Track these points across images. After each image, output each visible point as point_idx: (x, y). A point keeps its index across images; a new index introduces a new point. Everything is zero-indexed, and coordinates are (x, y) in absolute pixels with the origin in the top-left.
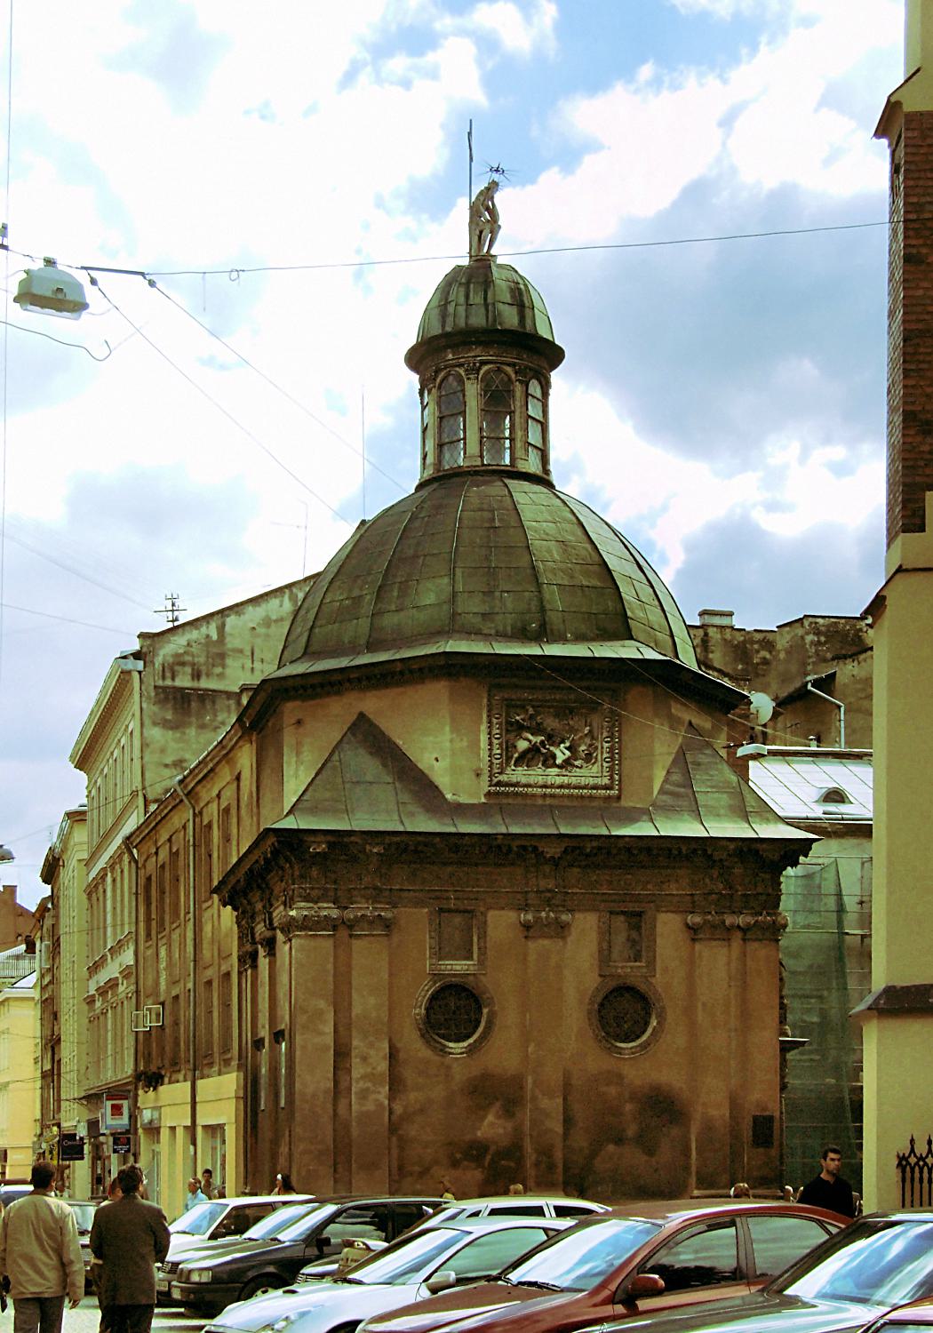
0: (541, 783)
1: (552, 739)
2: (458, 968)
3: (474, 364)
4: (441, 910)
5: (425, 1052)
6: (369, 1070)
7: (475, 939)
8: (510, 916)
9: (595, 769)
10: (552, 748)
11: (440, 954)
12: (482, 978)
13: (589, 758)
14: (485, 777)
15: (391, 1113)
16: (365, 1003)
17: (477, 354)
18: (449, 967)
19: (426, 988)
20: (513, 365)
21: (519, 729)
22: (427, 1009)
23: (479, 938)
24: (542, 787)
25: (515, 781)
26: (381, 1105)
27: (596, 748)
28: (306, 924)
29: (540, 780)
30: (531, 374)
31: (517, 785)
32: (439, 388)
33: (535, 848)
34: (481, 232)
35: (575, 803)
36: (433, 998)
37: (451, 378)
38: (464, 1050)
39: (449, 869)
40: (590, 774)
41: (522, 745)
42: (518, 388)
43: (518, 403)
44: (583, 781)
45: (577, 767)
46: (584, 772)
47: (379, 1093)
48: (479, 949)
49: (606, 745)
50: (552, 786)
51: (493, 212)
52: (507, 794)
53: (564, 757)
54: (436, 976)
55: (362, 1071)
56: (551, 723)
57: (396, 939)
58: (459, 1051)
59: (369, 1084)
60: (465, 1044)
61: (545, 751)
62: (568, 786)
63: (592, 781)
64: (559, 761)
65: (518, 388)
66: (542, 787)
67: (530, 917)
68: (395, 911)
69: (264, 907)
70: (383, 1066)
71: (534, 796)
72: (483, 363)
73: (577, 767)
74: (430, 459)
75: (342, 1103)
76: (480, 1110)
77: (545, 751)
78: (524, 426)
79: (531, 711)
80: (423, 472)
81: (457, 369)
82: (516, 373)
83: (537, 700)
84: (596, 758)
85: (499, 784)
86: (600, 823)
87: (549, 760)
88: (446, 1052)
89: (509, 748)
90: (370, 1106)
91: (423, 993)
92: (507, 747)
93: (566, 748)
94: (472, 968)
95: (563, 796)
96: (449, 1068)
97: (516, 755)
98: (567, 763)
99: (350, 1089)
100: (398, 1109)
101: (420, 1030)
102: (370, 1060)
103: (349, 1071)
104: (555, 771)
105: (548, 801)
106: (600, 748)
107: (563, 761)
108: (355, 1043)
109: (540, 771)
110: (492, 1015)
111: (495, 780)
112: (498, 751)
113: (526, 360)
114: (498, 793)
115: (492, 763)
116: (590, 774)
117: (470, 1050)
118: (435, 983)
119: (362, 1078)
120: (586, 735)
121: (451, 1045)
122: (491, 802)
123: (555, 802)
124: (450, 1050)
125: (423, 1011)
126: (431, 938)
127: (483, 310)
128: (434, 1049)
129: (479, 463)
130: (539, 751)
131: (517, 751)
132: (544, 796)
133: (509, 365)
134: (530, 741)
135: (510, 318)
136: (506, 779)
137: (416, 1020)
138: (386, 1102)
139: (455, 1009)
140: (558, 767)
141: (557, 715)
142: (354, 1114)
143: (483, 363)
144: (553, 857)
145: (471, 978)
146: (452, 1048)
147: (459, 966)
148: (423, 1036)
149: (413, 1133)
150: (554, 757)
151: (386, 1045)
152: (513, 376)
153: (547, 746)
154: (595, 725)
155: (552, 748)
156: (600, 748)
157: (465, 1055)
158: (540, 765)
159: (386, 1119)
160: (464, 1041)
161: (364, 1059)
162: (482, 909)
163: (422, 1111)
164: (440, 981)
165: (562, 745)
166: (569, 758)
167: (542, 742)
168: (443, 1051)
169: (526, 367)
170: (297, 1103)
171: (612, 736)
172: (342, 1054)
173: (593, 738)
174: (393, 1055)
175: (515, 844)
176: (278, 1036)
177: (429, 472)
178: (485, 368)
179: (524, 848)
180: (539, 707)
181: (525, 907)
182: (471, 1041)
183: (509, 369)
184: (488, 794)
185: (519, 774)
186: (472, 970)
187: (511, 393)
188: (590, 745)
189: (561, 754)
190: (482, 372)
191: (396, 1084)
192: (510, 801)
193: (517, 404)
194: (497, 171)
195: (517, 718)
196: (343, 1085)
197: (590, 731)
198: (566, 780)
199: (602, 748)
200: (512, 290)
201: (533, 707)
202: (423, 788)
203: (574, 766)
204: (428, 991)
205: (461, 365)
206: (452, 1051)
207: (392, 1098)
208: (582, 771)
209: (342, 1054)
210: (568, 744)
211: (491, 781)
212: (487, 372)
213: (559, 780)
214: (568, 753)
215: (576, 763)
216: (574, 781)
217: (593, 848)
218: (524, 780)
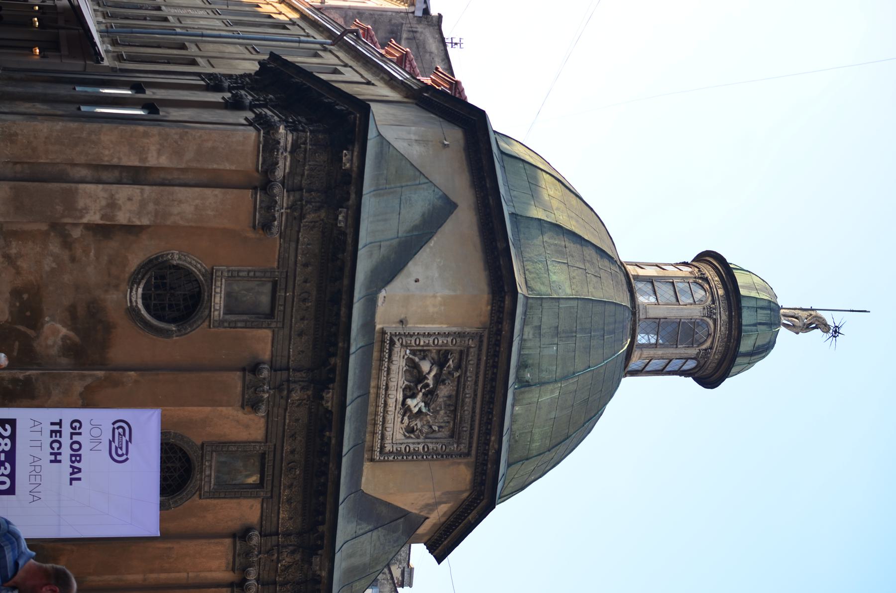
0: (391, 384)
1: (430, 396)
2: (217, 300)
3: (715, 314)
4: (275, 284)
5: (135, 261)
6: (120, 202)
7: (245, 317)
8: (265, 351)
9: (399, 436)
10: (421, 394)
11: (233, 277)
12: (206, 323)
13: (410, 430)
14: (400, 330)
15: (75, 225)
16: (188, 204)
17: (723, 316)
18: (218, 290)
20: (711, 348)
21: (441, 361)
22: (177, 267)
23: (246, 321)
24: (387, 385)
25: (394, 358)
26: (81, 217)
27: (418, 437)
28: (270, 146)
29: (392, 384)
30: (702, 362)
31: (390, 360)
33: (332, 381)
34: (796, 318)
35: (369, 418)
36: (188, 273)
37: (703, 293)
38: (134, 304)
39: (314, 293)
40: (395, 430)
41: (425, 366)
42: (693, 352)
43: (682, 351)
44: (389, 425)
45: (402, 419)
46: (398, 424)
47: (95, 213)
48: (236, 322)
49: (421, 447)
50: (387, 395)
51: (807, 328)
52: (382, 351)
53: (412, 407)
54: (210, 276)
55: (117, 196)
56: (444, 391)
57: (251, 234)
58: (134, 300)
59: (104, 203)
60: (140, 306)
61: (419, 387)
62: (385, 411)
63: (388, 434)
64: (409, 402)
65: (693, 352)
66: (387, 385)
67: (265, 374)
68: (277, 236)
69: (271, 100)
70: (122, 218)
71: (379, 378)
72: (715, 321)
73: (402, 419)
74: (641, 272)
75: (84, 172)
76: (72, 317)
77: (419, 388)
78: (665, 356)
79: (456, 374)
80: (631, 264)
81: (710, 298)
82: (706, 350)
83: (466, 381)
84: (409, 437)
85: (392, 343)
86: (352, 444)
87: (410, 392)
88: (133, 285)
89: (424, 354)
90: (81, 204)
91: (193, 262)
92: (424, 351)
93: (420, 409)
94: (216, 313)
95: (377, 406)
96: (117, 287)
97: (417, 359)
98: (406, 410)
99: (99, 182)
100: (76, 233)
101: (157, 258)
102: (130, 203)
103: (119, 182)
104: (400, 397)
105: (373, 391)
106: (419, 441)
109: (401, 383)
110: (166, 334)
111: (396, 340)
112: (422, 343)
113: (714, 357)
114: (383, 341)
115: (411, 336)
116: (395, 430)
118: (203, 275)
119: (112, 196)
120: (431, 427)
121: (140, 290)
122: (376, 335)
123: (372, 396)
124: (134, 289)
125: (175, 263)
126: (249, 271)
127: (753, 322)
128: (137, 272)
129: (642, 316)
130: (420, 382)
131: (421, 359)
132: (378, 387)
133: (712, 343)
134: (429, 373)
135: (746, 346)
136: (396, 350)
137: (168, 254)
138: (85, 220)
139: (175, 296)
140: (404, 403)
141: (449, 397)
142: (73, 185)
143: (715, 321)
144: (322, 398)
146: (137, 291)
147: (218, 301)
148: (151, 261)
149: (51, 247)
150: (413, 396)
151: (145, 221)
152: (704, 347)
153: (423, 390)
154: (438, 435)
155: (421, 394)
156: (419, 441)
158: (406, 383)
159: (66, 220)
160: (143, 304)
162: (274, 325)
163: (73, 259)
164: (206, 280)
165: (423, 404)
166: (411, 411)
167: (427, 385)
168: (134, 281)
169: (708, 358)
170: (88, 126)
171: (428, 453)
172: (136, 176)
173: (427, 433)
174: (132, 230)
175: (336, 361)
176: (151, 106)
177: (632, 271)
178: (711, 322)
179: (333, 370)
180: (460, 384)
181: (273, 368)
182: (143, 311)
183: (707, 344)
184: (383, 332)
185: (399, 364)
186: (215, 315)
187: (691, 345)
188: (421, 431)
189: (415, 404)
190: (708, 320)
191: (104, 231)
192: (376, 354)
193: (682, 351)
194: (835, 332)
195: (451, 362)
196: (105, 176)
197: (434, 431)
198: (391, 408)
199: (419, 443)
200: (763, 345)
201: (459, 377)
202: (391, 269)
203: (404, 415)
204: (196, 267)
205: (713, 302)
206: (134, 292)
207: (89, 227)
208: (399, 423)
209: (136, 176)
210: (424, 410)
211: (396, 335)
212: (708, 325)
213: (391, 402)
214: (415, 410)
215: (406, 418)
216: (390, 417)
217: (330, 438)
218: (394, 368)
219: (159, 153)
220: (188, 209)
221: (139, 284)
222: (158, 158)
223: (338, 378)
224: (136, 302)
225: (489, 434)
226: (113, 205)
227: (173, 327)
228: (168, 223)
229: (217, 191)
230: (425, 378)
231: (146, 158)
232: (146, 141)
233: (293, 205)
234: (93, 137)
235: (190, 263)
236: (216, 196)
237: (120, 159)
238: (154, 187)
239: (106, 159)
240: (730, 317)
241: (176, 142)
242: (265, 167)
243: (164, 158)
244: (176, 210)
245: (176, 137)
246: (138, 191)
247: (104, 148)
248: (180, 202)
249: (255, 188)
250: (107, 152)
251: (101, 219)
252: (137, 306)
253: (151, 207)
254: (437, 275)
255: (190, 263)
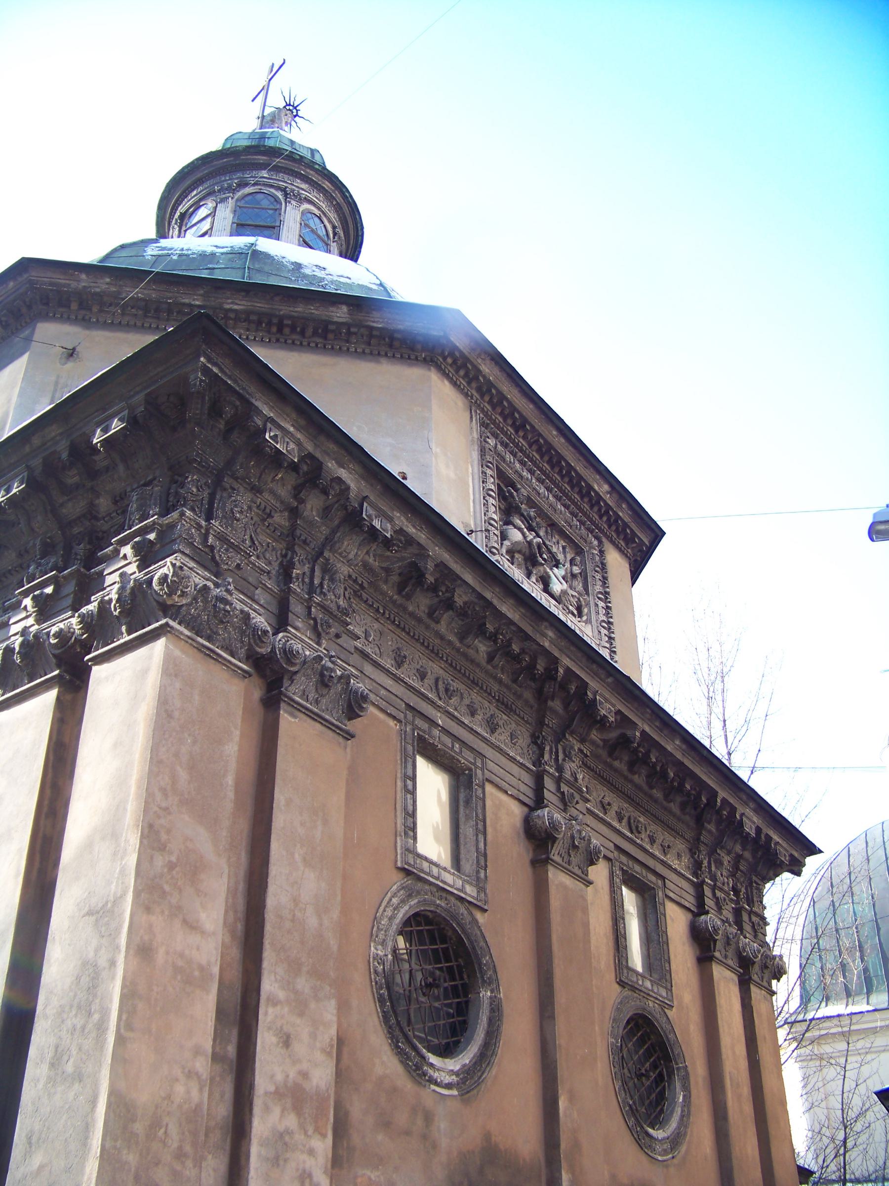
12: (479, 916)
19: (395, 901)
32: (237, 200)
58: (447, 1079)
59: (291, 1121)
60: (454, 1064)
70: (322, 1076)
91: (389, 912)
96: (428, 1118)
101: (381, 1000)
107: (564, 592)
108: (269, 985)
117: (464, 1081)
119: (278, 1094)
121: (433, 1059)
124: (436, 1075)
133: (330, 221)
145: (463, 910)
148: (386, 1018)
157: (455, 1092)
161: (286, 1041)
178: (306, 206)
182: (466, 1058)
199: (597, 605)
219: (192, 926)
220: (311, 884)
221: (423, 1057)
222: (203, 933)
223: (583, 675)
224: (452, 1072)
225: (590, 488)
226: (294, 1096)
227: (486, 994)
228: (335, 948)
229: (280, 797)
230: (530, 543)
231: (202, 968)
232: (160, 957)
233: (315, 629)
234: (139, 1127)
235: (391, 919)
236: (289, 802)
237: (197, 1051)
238: (265, 964)
239: (195, 1094)
240: (305, 179)
241: (171, 866)
242: (242, 653)
243: (203, 916)
244: (312, 921)
245: (159, 862)
246: (271, 1010)
247: (168, 1097)
248: (296, 901)
249: (273, 699)
250: (180, 1089)
251: (324, 1136)
252: (457, 1074)
253: (303, 984)
254: (390, 440)
255: (391, 919)
